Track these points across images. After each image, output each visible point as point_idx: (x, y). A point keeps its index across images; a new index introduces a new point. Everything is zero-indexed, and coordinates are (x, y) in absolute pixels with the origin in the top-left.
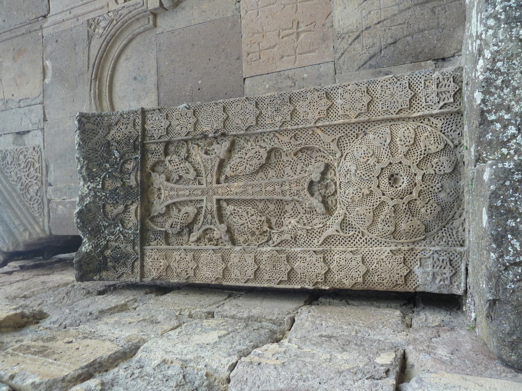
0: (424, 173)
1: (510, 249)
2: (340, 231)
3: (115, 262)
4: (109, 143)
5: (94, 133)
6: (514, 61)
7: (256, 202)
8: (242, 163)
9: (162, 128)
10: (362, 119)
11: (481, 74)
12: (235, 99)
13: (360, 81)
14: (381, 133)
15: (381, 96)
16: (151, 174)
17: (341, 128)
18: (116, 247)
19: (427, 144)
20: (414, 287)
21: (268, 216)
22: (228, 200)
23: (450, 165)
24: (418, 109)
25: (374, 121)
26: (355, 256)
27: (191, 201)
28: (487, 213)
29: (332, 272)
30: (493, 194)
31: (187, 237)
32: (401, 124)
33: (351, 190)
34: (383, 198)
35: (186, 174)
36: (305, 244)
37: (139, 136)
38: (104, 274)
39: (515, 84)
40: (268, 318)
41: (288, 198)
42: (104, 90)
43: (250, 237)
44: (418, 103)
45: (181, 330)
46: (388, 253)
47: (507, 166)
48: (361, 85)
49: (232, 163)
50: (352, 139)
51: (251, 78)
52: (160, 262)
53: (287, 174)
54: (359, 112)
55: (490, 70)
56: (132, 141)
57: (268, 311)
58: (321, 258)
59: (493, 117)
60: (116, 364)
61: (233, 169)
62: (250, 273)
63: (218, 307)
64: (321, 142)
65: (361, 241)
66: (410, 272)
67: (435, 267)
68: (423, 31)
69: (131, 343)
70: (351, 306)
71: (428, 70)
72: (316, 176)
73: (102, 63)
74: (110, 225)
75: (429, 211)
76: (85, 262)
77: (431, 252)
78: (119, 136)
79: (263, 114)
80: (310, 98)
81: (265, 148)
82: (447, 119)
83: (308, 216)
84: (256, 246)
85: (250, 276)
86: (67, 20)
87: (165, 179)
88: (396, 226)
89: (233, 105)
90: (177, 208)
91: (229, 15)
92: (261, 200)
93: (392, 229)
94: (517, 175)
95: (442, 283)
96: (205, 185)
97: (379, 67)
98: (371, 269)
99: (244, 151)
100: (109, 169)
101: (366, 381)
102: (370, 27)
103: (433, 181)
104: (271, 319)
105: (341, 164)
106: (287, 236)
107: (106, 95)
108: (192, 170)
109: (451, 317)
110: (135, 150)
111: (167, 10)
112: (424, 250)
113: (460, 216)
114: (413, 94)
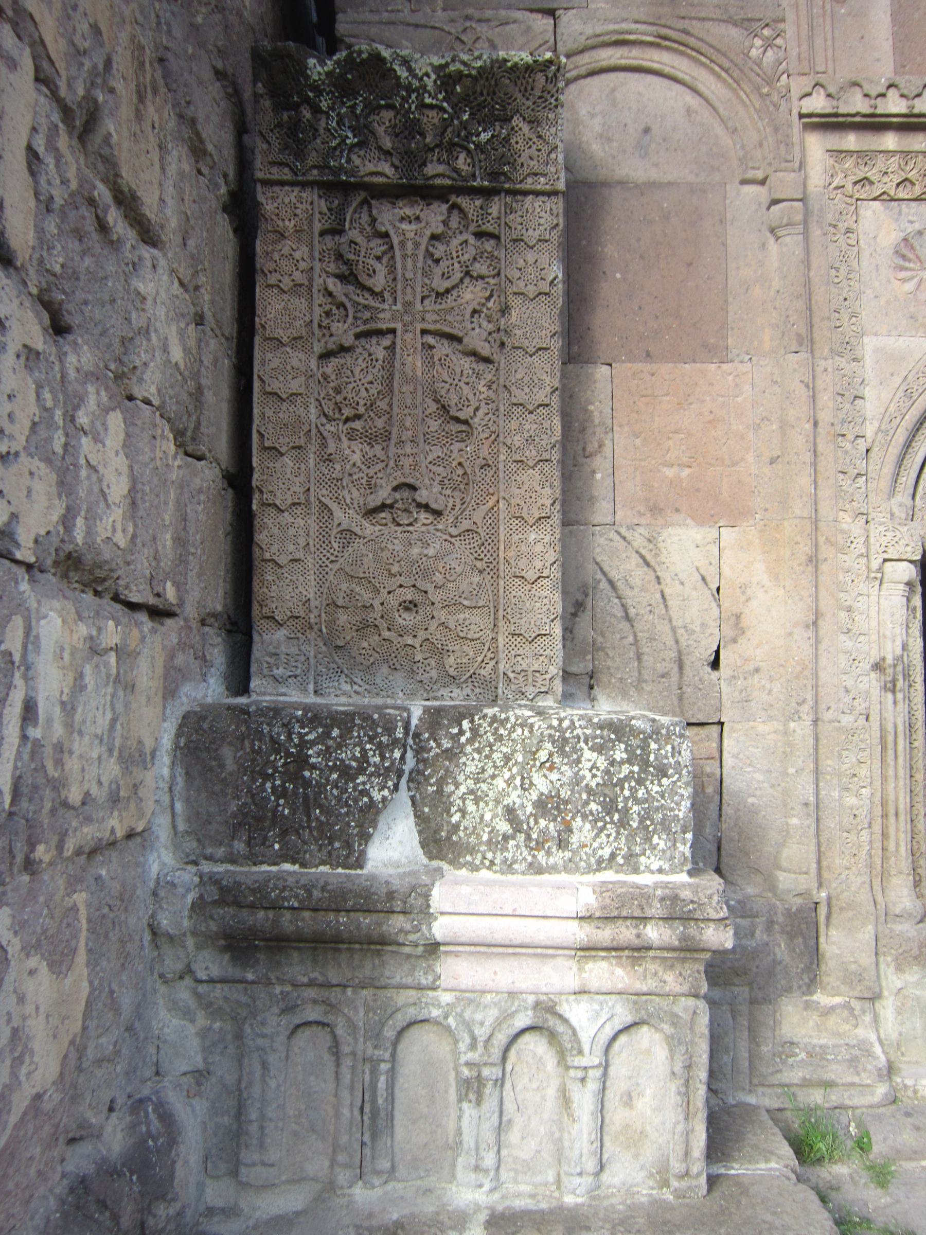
3: (289, 128)
4: (508, 120)
5: (526, 90)
9: (524, 231)
16: (447, 202)
18: (316, 130)
19: (458, 654)
27: (395, 279)
38: (267, 103)
41: (392, 450)
43: (332, 385)
49: (454, 358)
54: (513, 564)
56: (506, 168)
62: (275, 386)
65: (324, 559)
72: (423, 496)
74: (357, 118)
75: (363, 652)
83: (364, 481)
90: (384, 253)
92: (390, 405)
93: (340, 602)
95: (265, 665)
100: (458, 118)
105: (439, 534)
106: (332, 447)
108: (447, 284)
110: (489, 174)
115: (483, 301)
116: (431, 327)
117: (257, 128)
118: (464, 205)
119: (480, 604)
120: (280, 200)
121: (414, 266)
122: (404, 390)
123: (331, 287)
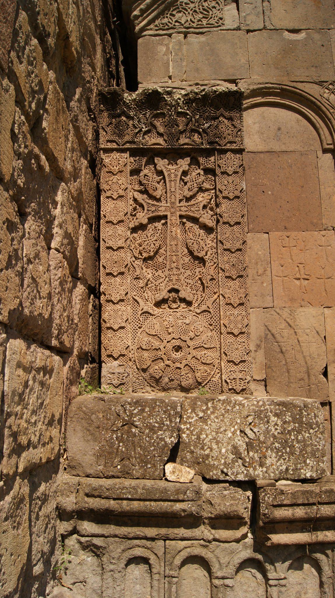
1: (133, 408)
2: (143, 311)
4: (218, 118)
10: (223, 328)
18: (128, 125)
27: (166, 192)
34: (165, 341)
39: (226, 415)
43: (137, 242)
49: (195, 228)
54: (228, 326)
55: (235, 403)
56: (217, 140)
59: (210, 405)
62: (110, 243)
68: (288, 372)
72: (182, 294)
75: (156, 371)
78: (222, 128)
90: (161, 180)
91: (324, 221)
93: (144, 347)
95: (108, 378)
96: (179, 205)
99: (205, 237)
102: (296, 335)
108: (191, 193)
113: (153, 391)
116: (183, 213)
119: (212, 346)
121: (175, 185)
123: (136, 196)
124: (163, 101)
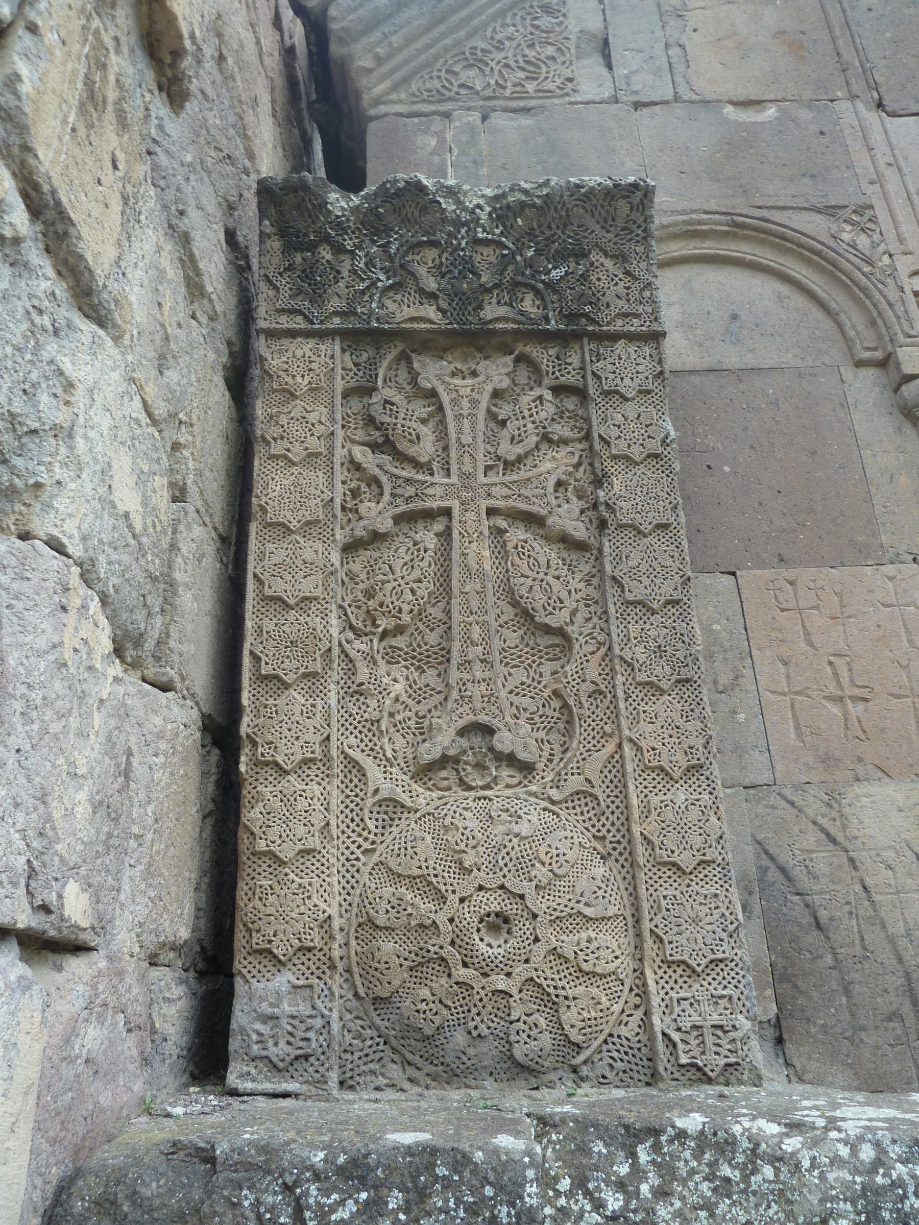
0: (511, 996)
1: (335, 1196)
2: (377, 798)
3: (304, 271)
4: (584, 255)
5: (606, 221)
6: (775, 1207)
7: (445, 601)
8: (536, 569)
9: (618, 381)
11: (745, 1130)
12: (686, 550)
13: (728, 846)
14: (607, 895)
15: (694, 894)
16: (511, 353)
17: (617, 801)
18: (338, 272)
19: (582, 1003)
20: (244, 971)
21: (411, 630)
22: (450, 535)
23: (531, 1057)
24: (662, 982)
25: (633, 877)
26: (317, 834)
27: (446, 448)
28: (418, 1144)
29: (280, 779)
30: (464, 1156)
31: (361, 440)
32: (627, 941)
33: (473, 824)
34: (454, 899)
35: (509, 437)
36: (346, 715)
37: (600, 325)
38: (276, 244)
39: (723, 1207)
40: (171, 630)
41: (454, 675)
42: (708, 244)
43: (361, 586)
44: (676, 982)
45: (143, 424)
46: (324, 912)
47: (528, 1189)
48: (719, 847)
49: (535, 544)
50: (593, 826)
51: (735, 590)
52: (303, 376)
53: (510, 674)
54: (657, 842)
55: (753, 1151)
56: (587, 309)
57: (189, 630)
58: (313, 752)
59: (643, 1157)
60: (64, 271)
61: (523, 547)
62: (277, 587)
63: (198, 511)
64: (586, 755)
65: (353, 847)
66: (279, 964)
67: (292, 1022)
68: (847, 992)
69: (113, 307)
70: (200, 823)
71: (754, 1005)
72: (504, 741)
73: (772, 238)
74: (391, 258)
75: (423, 1006)
76: (303, 200)
77: (326, 1012)
78: (599, 280)
79: (652, 618)
80: (689, 728)
81: (572, 622)
82: (639, 1049)
83: (412, 723)
84: (340, 602)
85: (270, 587)
86: (871, 157)
87: (498, 387)
88: (387, 928)
89: (673, 547)
90: (431, 415)
92: (448, 613)
93: (381, 921)
94: (509, 1214)
95: (254, 1037)
97: (762, 890)
98: (287, 870)
99: (565, 572)
100: (521, 255)
101: (23, 859)
102: (856, 868)
103: (492, 1016)
104: (168, 636)
106: (363, 672)
107: (695, 248)
108: (519, 450)
109: (175, 1057)
110: (565, 316)
111: (896, 391)
112: (332, 994)
113: (411, 1080)
114: (699, 969)
115: (571, 469)
117: (262, 272)
118: (535, 354)
120: (290, 353)
122: (467, 589)
124: (437, 211)
